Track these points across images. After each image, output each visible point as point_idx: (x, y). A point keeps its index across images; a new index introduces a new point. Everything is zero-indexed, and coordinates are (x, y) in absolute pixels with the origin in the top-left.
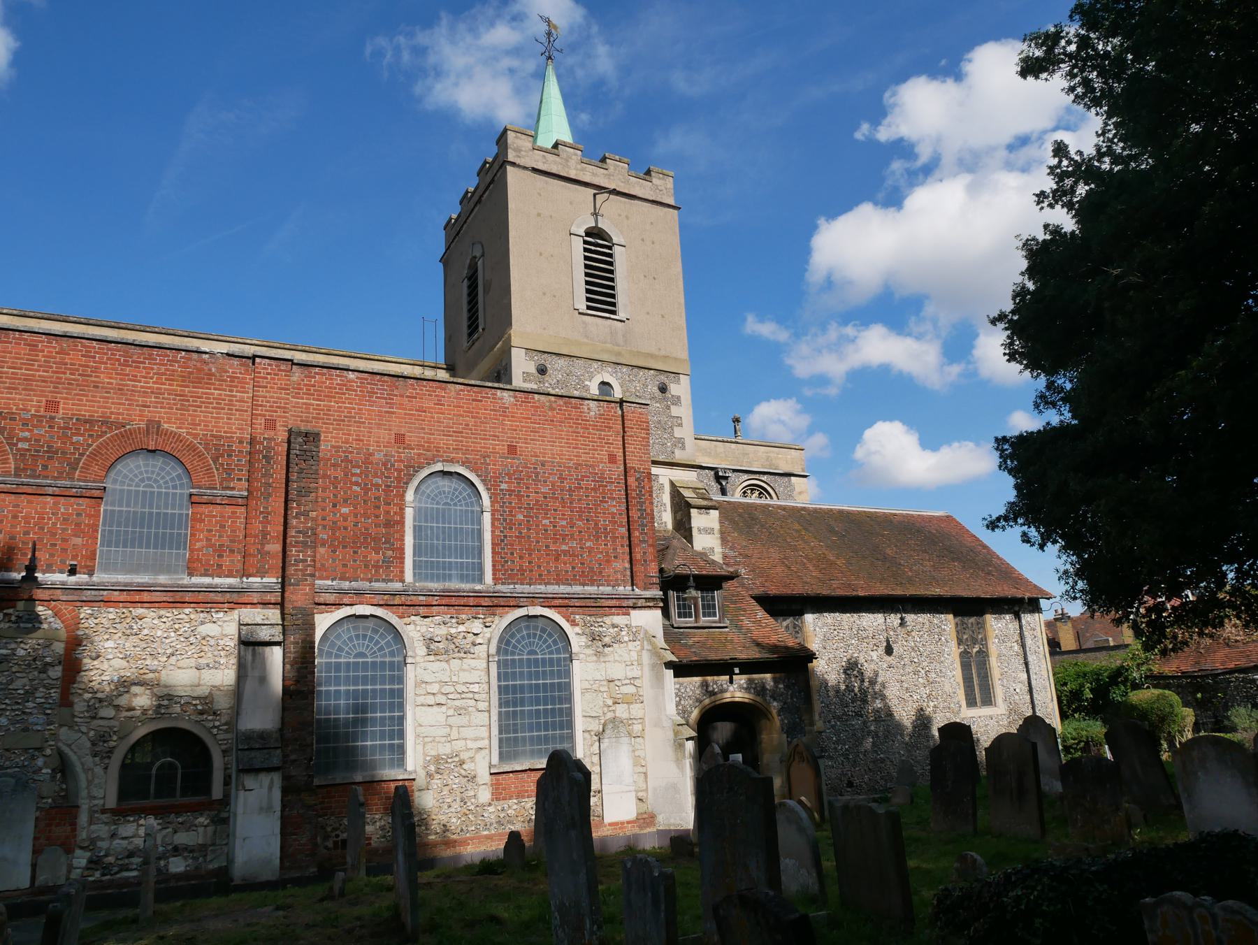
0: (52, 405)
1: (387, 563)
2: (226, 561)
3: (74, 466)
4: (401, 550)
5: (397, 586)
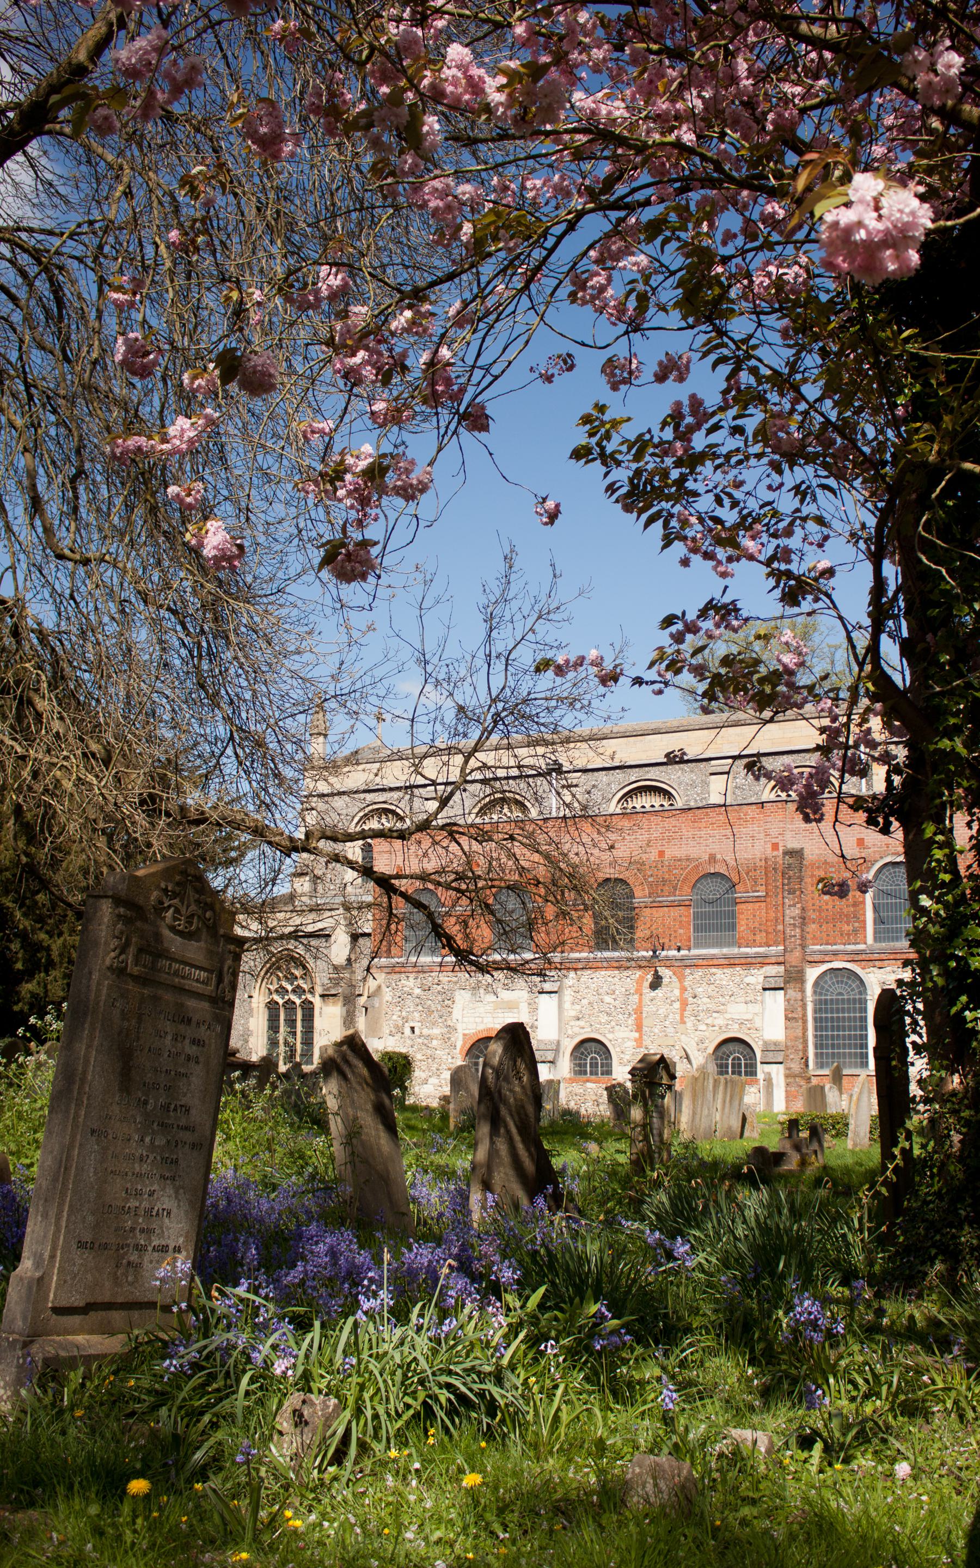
0: (661, 854)
1: (855, 931)
2: (758, 938)
3: (675, 888)
4: (864, 922)
5: (862, 947)
